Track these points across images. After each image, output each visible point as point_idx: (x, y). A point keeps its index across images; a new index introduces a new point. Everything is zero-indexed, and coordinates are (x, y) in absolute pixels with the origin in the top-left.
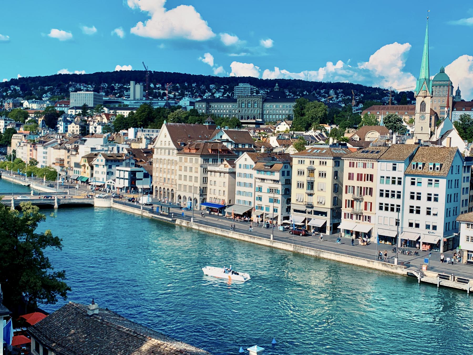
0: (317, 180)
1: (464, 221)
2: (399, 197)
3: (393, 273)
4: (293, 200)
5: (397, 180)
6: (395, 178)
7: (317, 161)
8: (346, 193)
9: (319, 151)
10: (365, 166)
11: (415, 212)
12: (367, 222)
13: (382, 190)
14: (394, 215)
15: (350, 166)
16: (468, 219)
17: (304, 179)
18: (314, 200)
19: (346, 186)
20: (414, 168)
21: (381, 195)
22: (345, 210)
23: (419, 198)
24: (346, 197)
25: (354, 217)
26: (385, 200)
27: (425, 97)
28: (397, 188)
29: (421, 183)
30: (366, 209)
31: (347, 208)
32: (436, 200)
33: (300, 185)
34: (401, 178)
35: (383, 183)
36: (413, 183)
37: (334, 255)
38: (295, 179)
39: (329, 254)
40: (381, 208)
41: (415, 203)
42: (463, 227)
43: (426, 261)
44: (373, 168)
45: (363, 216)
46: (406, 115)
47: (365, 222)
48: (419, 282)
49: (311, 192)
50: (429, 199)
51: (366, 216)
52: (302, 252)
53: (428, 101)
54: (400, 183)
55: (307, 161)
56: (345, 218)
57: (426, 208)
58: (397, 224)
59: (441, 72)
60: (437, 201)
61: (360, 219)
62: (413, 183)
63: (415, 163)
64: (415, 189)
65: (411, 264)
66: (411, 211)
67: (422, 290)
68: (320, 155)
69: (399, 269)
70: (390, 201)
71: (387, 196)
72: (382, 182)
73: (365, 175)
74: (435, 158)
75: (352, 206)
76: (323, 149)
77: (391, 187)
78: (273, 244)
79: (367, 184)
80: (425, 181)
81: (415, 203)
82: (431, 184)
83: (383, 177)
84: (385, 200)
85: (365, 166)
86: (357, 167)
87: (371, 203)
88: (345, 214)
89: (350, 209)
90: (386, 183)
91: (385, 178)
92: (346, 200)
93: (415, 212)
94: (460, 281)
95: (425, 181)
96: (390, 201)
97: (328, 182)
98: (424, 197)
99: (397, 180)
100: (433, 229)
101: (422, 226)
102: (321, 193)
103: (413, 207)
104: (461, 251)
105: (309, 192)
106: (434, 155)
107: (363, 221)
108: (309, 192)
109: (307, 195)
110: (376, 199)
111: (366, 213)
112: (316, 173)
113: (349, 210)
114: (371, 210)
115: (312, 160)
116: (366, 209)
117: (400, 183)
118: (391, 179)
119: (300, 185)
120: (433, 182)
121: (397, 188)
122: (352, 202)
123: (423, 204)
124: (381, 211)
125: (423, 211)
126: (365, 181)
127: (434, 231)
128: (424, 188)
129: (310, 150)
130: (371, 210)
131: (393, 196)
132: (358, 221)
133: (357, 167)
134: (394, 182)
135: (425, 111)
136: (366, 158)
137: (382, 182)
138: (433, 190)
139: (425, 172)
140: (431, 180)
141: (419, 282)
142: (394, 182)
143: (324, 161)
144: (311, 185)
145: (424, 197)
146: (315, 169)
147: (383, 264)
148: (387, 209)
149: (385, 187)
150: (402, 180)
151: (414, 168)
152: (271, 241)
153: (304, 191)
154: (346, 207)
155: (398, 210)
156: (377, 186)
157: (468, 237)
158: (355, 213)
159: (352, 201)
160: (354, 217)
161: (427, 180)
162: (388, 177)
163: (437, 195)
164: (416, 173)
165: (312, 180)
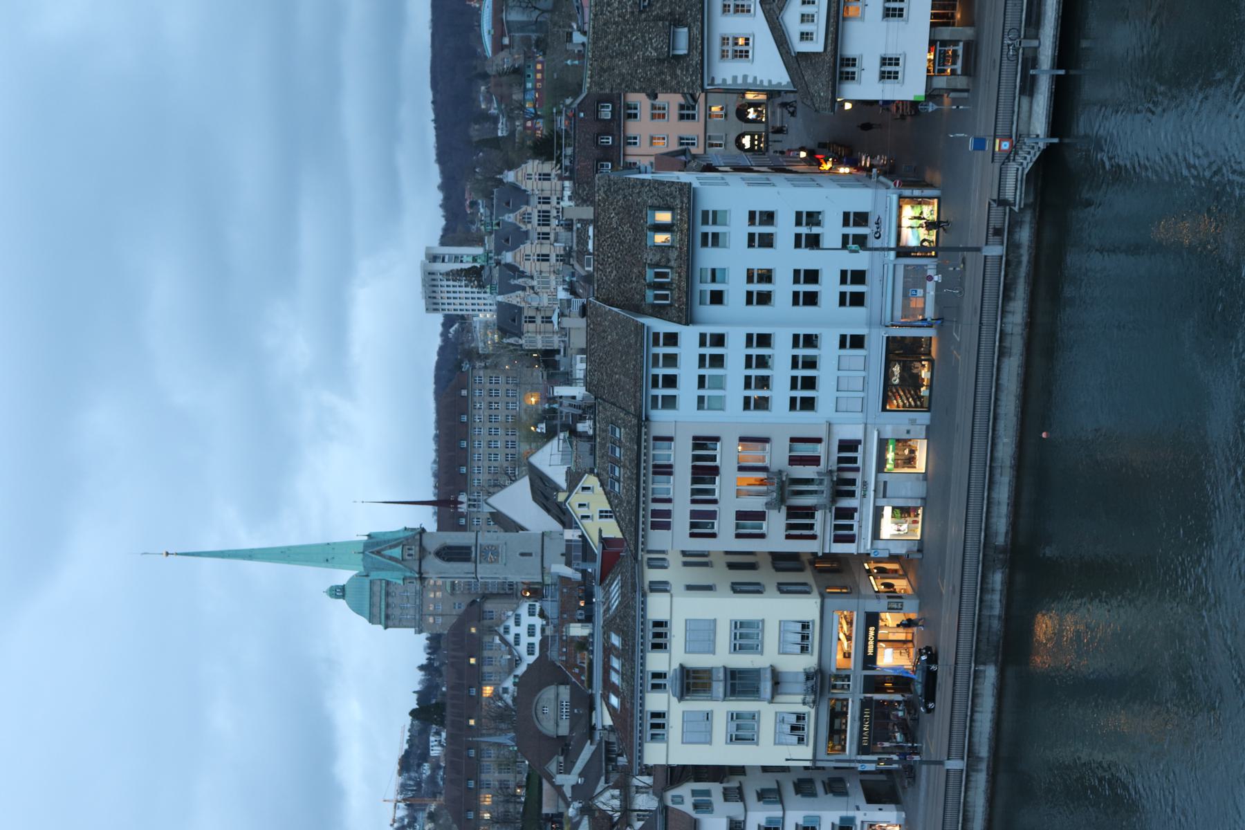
0: (722, 657)
1: (834, 87)
2: (764, 340)
3: (1035, 262)
4: (801, 754)
5: (709, 351)
6: (702, 357)
7: (656, 662)
8: (762, 536)
9: (616, 663)
10: (665, 470)
11: (815, 230)
12: (859, 455)
13: (747, 400)
14: (828, 351)
15: (667, 526)
16: (825, 77)
17: (721, 709)
18: (798, 664)
19: (738, 536)
20: (665, 297)
21: (762, 404)
22: (822, 542)
23: (766, 276)
24: (775, 536)
25: (846, 503)
26: (780, 392)
27: (423, 550)
28: (735, 351)
29: (713, 271)
30: (815, 461)
31: (817, 530)
32: (769, 217)
33: (743, 732)
34: (703, 337)
35: (721, 399)
36: (717, 298)
37: (996, 488)
38: (720, 753)
39: (995, 509)
40: (808, 404)
41: (783, 288)
42: (853, 92)
43: (980, 144)
44: (670, 439)
45: (840, 469)
46: (480, 691)
47: (859, 463)
48: (1056, 140)
49: (768, 675)
50: (767, 241)
51: (840, 460)
52: (996, 625)
53: (432, 545)
54: (719, 340)
55: (656, 701)
56: (851, 539)
57: (798, 250)
58: (857, 342)
59: (343, 597)
60: (770, 271)
61: (853, 482)
62: (717, 298)
63: (650, 294)
64: (736, 288)
65: (995, 197)
66: (811, 299)
67: (1085, 124)
68: (630, 654)
69: (1017, 236)
70: (781, 373)
71: (764, 382)
72: (719, 405)
73: (693, 501)
74: (629, 237)
75: (809, 512)
76: (608, 650)
77: (735, 369)
78: (980, 759)
79: (727, 455)
80: (708, 258)
81: (783, 288)
82: (716, 235)
83: (701, 399)
84: (780, 392)
85: (665, 470)
86: (669, 501)
87: (793, 440)
88: (838, 539)
89: (819, 515)
90: (721, 388)
91: (702, 392)
92: (788, 537)
93: (815, 230)
94: (1028, 87)
95: (708, 258)
96: (781, 373)
97: (727, 608)
98: (760, 258)
99: (709, 351)
100: (866, 225)
101: (858, 260)
102: (771, 639)
103: (798, 237)
104: (932, 94)
105: (766, 687)
106: (622, 243)
107: (857, 470)
108: (766, 687)
109: (779, 698)
110: (780, 419)
111: (827, 454)
112: (698, 661)
113: (822, 522)
114: (819, 440)
115: (650, 681)
116: (815, 461)
117: (719, 340)
118: (708, 372)
119: (743, 732)
120: (710, 229)
121: (735, 351)
122: (793, 512)
123: (785, 259)
124: (819, 404)
125: (808, 259)
126: (715, 502)
127: (872, 220)
128: (732, 259)
129: (614, 701)
130: (819, 440)
131: (763, 362)
132: (858, 489)
133: (669, 501)
134: (718, 361)
135: (469, 548)
136: (638, 474)
137: (719, 405)
138: (737, 229)
139: (679, 257)
140: (705, 235)
141: (1056, 140)
142: (718, 361)
143: (650, 630)
144: (740, 683)
145: (760, 258)
146: (682, 667)
147: (1007, 296)
148: (810, 383)
149: (735, 391)
150: (709, 330)
151: (665, 297)
152: (971, 768)
153: (767, 713)
154: (814, 537)
155: (810, 341)
156: (730, 419)
157: (884, 76)
158: (833, 501)
159: (789, 516)
160: (846, 503)
161: (705, 249)
162: (702, 381)
163: (752, 215)
164: (683, 284)
165: (721, 676)
